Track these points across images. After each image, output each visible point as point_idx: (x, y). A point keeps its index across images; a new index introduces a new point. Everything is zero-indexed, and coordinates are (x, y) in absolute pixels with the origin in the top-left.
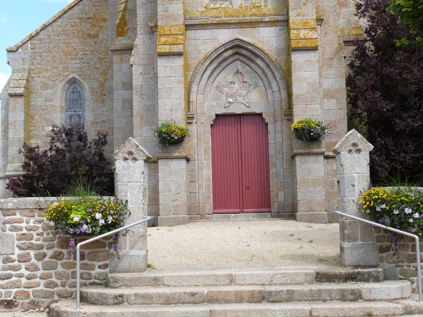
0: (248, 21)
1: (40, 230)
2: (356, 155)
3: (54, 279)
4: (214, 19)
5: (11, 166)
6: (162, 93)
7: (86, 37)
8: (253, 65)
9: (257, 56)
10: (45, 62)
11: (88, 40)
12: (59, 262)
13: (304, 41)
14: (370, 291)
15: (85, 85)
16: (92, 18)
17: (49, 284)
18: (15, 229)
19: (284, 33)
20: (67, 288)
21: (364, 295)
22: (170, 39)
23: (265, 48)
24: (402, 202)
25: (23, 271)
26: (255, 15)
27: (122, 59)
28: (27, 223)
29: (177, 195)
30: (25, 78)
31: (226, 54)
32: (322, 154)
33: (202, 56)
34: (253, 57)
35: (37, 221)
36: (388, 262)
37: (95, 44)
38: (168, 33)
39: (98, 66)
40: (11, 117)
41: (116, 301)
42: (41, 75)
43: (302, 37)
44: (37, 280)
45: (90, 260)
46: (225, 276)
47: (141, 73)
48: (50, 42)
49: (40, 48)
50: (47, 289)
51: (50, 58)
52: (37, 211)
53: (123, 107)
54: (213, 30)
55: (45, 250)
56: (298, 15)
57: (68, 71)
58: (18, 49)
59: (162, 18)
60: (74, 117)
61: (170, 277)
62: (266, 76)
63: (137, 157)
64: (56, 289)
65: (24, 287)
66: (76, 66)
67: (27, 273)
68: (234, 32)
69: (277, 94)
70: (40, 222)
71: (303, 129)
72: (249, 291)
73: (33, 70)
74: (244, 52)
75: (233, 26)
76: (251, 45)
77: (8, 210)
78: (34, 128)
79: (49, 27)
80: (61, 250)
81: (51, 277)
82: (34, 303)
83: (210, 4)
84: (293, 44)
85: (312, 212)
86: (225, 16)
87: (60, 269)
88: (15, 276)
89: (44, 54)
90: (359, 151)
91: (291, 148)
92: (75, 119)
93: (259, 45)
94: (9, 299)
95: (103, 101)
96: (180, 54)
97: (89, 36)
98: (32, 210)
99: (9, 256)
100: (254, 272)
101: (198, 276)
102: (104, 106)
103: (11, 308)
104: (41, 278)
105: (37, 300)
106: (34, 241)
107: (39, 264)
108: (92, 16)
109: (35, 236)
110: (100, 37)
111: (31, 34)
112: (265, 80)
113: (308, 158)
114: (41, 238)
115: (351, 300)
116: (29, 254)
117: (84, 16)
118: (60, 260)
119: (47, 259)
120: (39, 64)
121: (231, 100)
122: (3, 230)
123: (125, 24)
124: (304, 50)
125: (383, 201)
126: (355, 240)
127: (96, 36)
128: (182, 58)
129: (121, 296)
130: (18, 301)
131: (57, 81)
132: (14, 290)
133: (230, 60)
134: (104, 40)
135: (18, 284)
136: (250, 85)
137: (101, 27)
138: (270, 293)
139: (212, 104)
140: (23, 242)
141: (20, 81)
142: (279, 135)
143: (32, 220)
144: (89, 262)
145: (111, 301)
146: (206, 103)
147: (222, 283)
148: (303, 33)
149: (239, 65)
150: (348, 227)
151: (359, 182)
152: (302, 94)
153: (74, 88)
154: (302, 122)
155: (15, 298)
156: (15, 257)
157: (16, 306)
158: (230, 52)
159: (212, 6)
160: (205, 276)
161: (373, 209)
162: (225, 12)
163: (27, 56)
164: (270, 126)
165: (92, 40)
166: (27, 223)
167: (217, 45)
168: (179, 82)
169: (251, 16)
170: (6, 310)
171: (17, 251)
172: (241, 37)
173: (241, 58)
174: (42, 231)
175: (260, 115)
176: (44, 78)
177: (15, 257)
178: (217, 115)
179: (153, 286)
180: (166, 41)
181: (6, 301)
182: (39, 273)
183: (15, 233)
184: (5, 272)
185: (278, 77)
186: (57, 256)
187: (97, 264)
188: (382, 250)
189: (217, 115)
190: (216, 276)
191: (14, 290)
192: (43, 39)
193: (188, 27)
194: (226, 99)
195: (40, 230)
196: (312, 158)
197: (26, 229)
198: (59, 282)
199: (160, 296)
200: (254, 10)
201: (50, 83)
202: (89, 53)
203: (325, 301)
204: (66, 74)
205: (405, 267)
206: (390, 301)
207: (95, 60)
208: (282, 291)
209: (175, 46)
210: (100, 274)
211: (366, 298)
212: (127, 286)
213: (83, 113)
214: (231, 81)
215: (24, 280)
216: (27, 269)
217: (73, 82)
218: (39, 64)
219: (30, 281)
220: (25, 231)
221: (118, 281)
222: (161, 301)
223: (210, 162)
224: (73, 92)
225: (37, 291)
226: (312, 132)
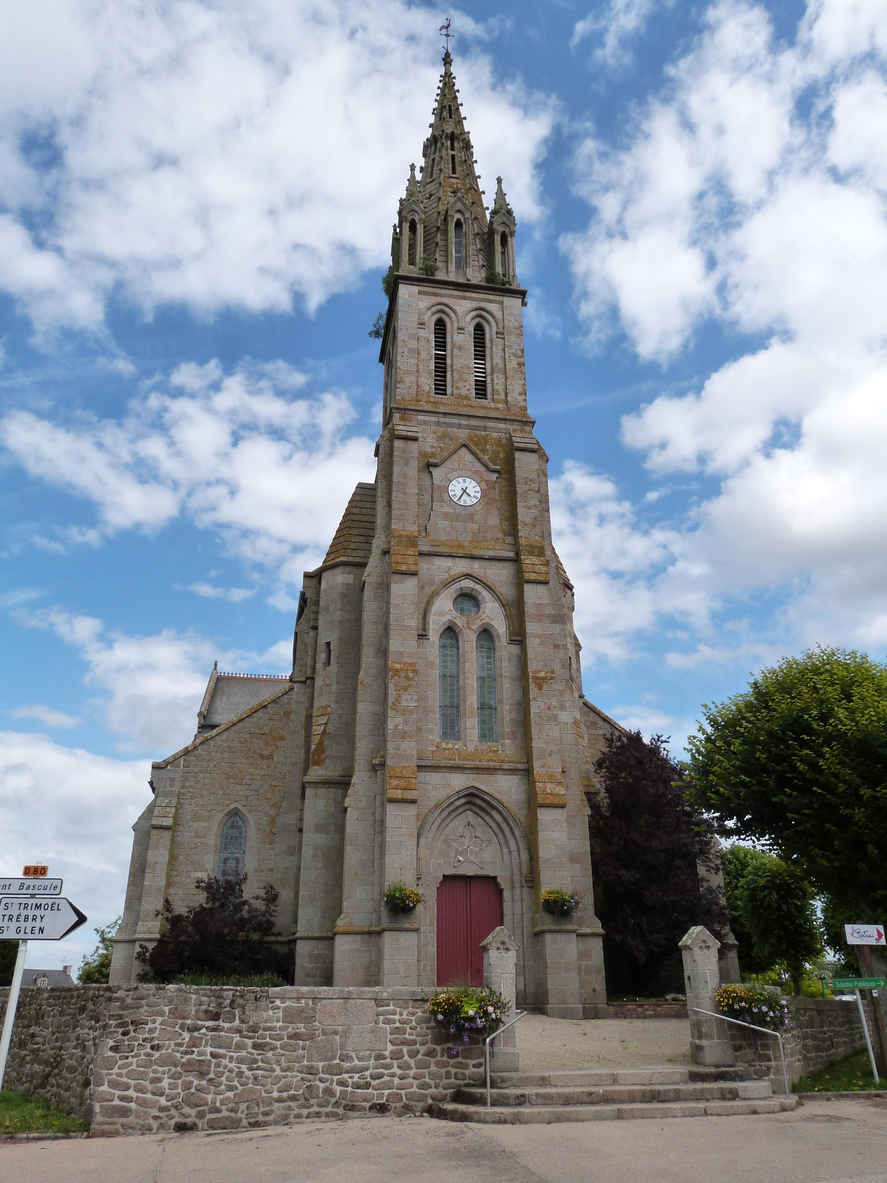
0: (486, 767)
1: (414, 1024)
2: (705, 951)
3: (427, 1080)
4: (446, 761)
5: (143, 925)
6: (390, 847)
7: (256, 757)
8: (487, 818)
9: (493, 807)
10: (200, 785)
11: (259, 762)
12: (433, 1060)
13: (551, 797)
14: (745, 1089)
15: (251, 819)
16: (268, 735)
17: (423, 1085)
18: (388, 1022)
19: (525, 784)
20: (441, 1089)
21: (740, 1093)
22: (402, 783)
23: (504, 799)
24: (759, 1000)
25: (395, 1070)
26: (492, 761)
27: (316, 794)
28: (401, 1015)
29: (406, 979)
30: (174, 805)
31: (458, 803)
32: (574, 932)
33: (432, 804)
34: (488, 809)
35: (410, 1013)
36: (742, 1062)
37: (268, 767)
38: (400, 775)
39: (269, 796)
40: (151, 856)
41: (518, 1101)
42: (193, 801)
43: (549, 791)
44: (410, 1080)
45: (464, 1058)
46: (608, 1075)
47: (358, 818)
48: (210, 760)
49: (196, 766)
50: (421, 1091)
51: (207, 781)
52: (411, 1002)
53: (315, 856)
54: (446, 774)
55: (418, 1046)
56: (543, 766)
57: (229, 799)
58: (167, 766)
59: (392, 757)
60: (230, 861)
61: (557, 1076)
62: (502, 831)
63: (510, 947)
64: (429, 1090)
65: (397, 1089)
66: (241, 793)
67: (399, 1072)
68: (469, 779)
69: (515, 855)
70: (413, 1015)
71: (555, 901)
72: (640, 1090)
73: (183, 794)
74: (478, 802)
75: (468, 772)
76: (489, 794)
77: (382, 1000)
78: (176, 873)
79: (210, 741)
80: (435, 1046)
81: (425, 1078)
82: (407, 1108)
83: (441, 743)
84: (540, 800)
85: (563, 1005)
86: (459, 759)
87: (433, 1068)
88: (388, 1075)
89: (201, 775)
90: (708, 947)
91: (534, 924)
92: (232, 864)
93: (498, 796)
94: (381, 1102)
95: (272, 842)
96: (414, 802)
97: (261, 756)
98: (406, 1001)
99: (382, 1052)
100: (635, 1071)
101: (583, 1076)
102: (273, 849)
103: (383, 1112)
104: (414, 1078)
105: (411, 1103)
106: (406, 1036)
107: (412, 1062)
108: (267, 731)
109: (408, 1030)
110: (275, 759)
111: (187, 748)
112: (501, 836)
113: (558, 936)
114: (414, 1032)
115: (730, 1099)
116: (401, 1050)
117: (257, 731)
118: (432, 1058)
119: (419, 1056)
120: (192, 786)
121: (461, 858)
122: (377, 1022)
123: (323, 752)
124: (552, 807)
125: (742, 999)
126: (712, 1038)
127: (270, 757)
128: (416, 806)
129: (523, 1096)
130: (391, 1104)
131: (214, 812)
132: (386, 1092)
133: (461, 810)
134: (279, 763)
135: (391, 1085)
136: (482, 841)
137: (277, 747)
138: (659, 1092)
139: (439, 861)
140: (396, 1036)
141: (168, 809)
142: (518, 905)
143: (405, 1012)
144: (464, 1061)
145: (512, 1101)
146: (432, 860)
147: (606, 1083)
148: (550, 787)
149: (470, 816)
150: (705, 1025)
151: (710, 978)
152: (550, 859)
153: (233, 822)
154: (551, 893)
155: (387, 1101)
156: (387, 1053)
157: (389, 1111)
158: (463, 801)
159: (444, 745)
160: (590, 1075)
161: (730, 1006)
162: (459, 754)
163: (177, 776)
164: (506, 894)
165: (264, 762)
166: (401, 1015)
167: (449, 792)
168: (410, 835)
169: (488, 761)
170: (379, 1115)
171: (390, 1047)
172: (476, 785)
173: (473, 808)
174: (415, 1025)
175: (495, 878)
176: (196, 806)
177: (387, 1053)
178: (444, 876)
179: (541, 1086)
180: (397, 785)
181: (378, 1104)
182: (412, 1073)
183: (388, 1026)
184: (377, 1071)
185: (517, 833)
186: (431, 1054)
187: (472, 1062)
188: (737, 1048)
189: (444, 876)
190: (600, 1075)
191: (386, 1092)
192: (202, 756)
193: (420, 768)
194: (456, 857)
195: (414, 1024)
196: (564, 937)
197: (399, 1022)
198: (432, 1083)
199: (560, 1096)
200: (491, 755)
201: (204, 813)
202: (258, 777)
203: (708, 1100)
204: (226, 802)
205: (758, 1067)
206: (761, 1099)
207: (266, 787)
208: (669, 1090)
209: (409, 792)
210: (475, 1074)
211: (743, 1097)
212: (515, 1086)
213: (242, 857)
214: (460, 834)
215: (396, 1081)
216: (399, 1067)
217: (235, 813)
218: (192, 786)
219: (402, 1081)
220: (398, 1025)
221: (506, 1081)
222: (561, 1102)
223: (435, 936)
224: (232, 827)
225: (410, 1093)
226: (566, 906)
